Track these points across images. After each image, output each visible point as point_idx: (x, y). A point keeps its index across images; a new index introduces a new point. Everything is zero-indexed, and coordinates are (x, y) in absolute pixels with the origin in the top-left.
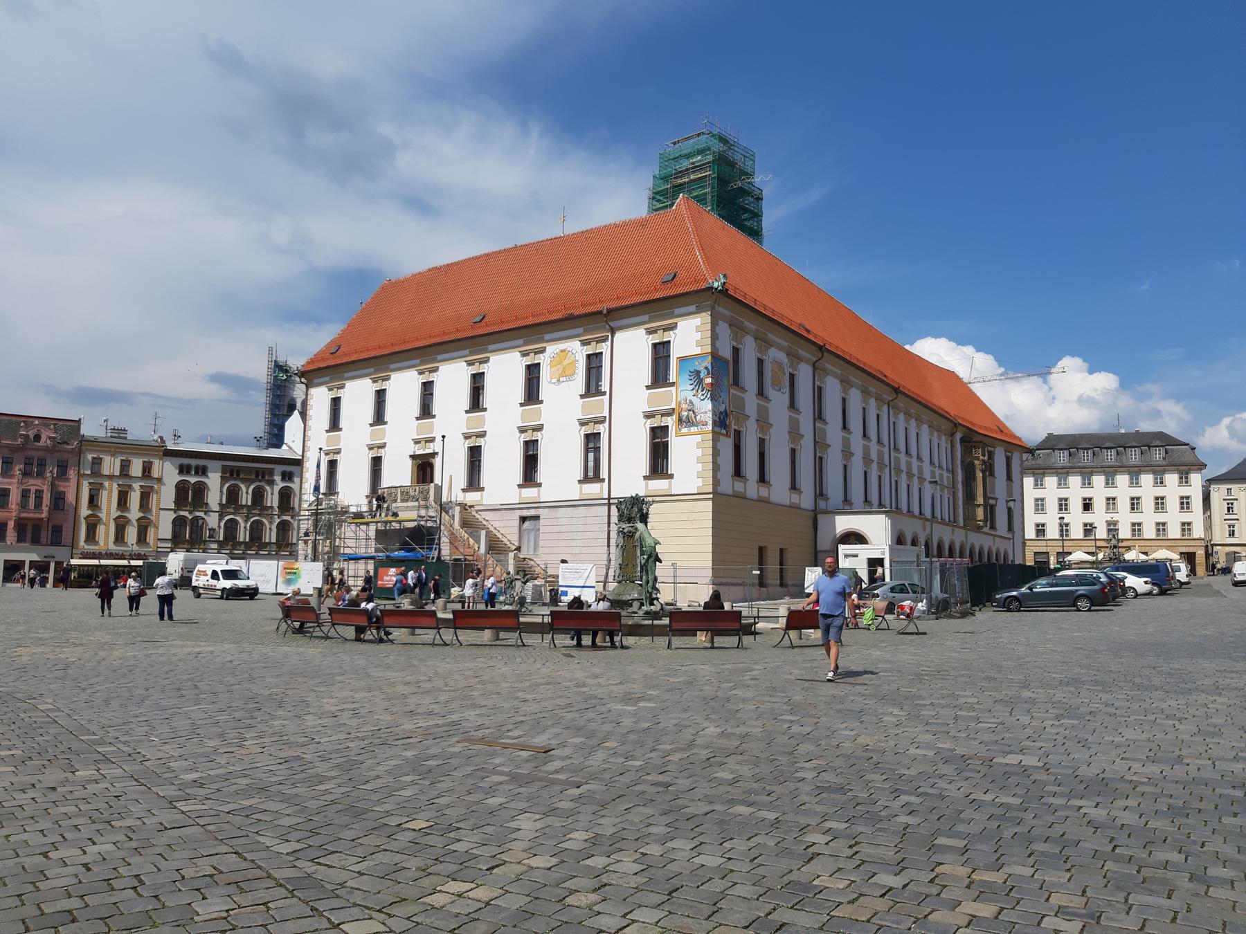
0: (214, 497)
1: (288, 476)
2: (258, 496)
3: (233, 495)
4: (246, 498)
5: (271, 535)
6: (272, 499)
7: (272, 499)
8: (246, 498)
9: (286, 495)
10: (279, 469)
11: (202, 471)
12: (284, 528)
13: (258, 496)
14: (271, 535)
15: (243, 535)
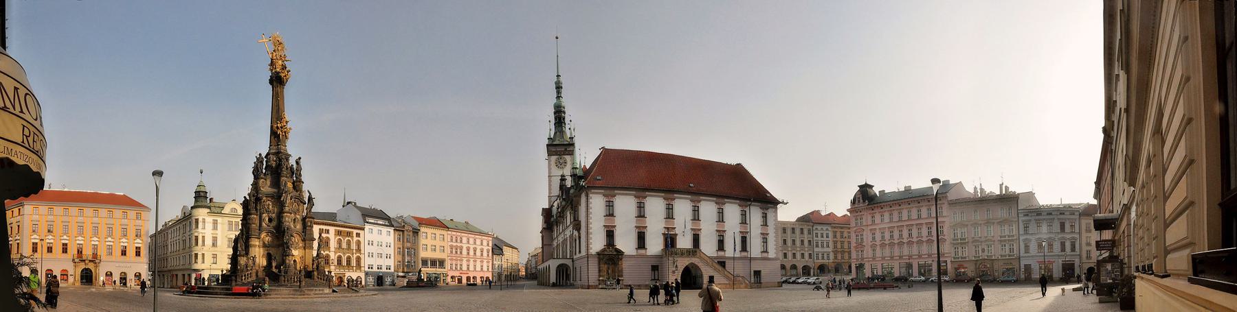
0: (333, 244)
1: (358, 235)
2: (349, 243)
3: (340, 242)
4: (344, 245)
5: (354, 263)
6: (354, 246)
7: (354, 246)
8: (344, 245)
9: (358, 243)
10: (355, 231)
11: (327, 232)
12: (358, 259)
13: (349, 243)
14: (354, 263)
15: (344, 263)
